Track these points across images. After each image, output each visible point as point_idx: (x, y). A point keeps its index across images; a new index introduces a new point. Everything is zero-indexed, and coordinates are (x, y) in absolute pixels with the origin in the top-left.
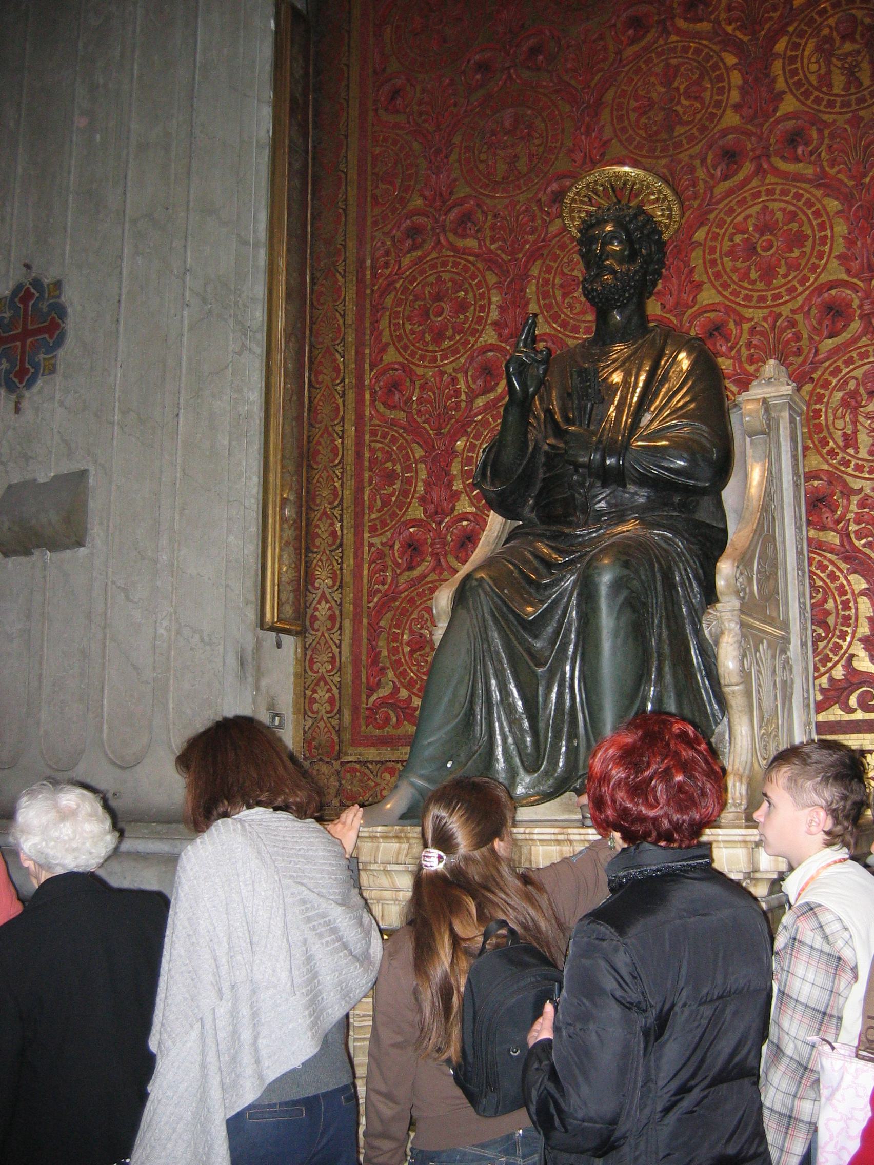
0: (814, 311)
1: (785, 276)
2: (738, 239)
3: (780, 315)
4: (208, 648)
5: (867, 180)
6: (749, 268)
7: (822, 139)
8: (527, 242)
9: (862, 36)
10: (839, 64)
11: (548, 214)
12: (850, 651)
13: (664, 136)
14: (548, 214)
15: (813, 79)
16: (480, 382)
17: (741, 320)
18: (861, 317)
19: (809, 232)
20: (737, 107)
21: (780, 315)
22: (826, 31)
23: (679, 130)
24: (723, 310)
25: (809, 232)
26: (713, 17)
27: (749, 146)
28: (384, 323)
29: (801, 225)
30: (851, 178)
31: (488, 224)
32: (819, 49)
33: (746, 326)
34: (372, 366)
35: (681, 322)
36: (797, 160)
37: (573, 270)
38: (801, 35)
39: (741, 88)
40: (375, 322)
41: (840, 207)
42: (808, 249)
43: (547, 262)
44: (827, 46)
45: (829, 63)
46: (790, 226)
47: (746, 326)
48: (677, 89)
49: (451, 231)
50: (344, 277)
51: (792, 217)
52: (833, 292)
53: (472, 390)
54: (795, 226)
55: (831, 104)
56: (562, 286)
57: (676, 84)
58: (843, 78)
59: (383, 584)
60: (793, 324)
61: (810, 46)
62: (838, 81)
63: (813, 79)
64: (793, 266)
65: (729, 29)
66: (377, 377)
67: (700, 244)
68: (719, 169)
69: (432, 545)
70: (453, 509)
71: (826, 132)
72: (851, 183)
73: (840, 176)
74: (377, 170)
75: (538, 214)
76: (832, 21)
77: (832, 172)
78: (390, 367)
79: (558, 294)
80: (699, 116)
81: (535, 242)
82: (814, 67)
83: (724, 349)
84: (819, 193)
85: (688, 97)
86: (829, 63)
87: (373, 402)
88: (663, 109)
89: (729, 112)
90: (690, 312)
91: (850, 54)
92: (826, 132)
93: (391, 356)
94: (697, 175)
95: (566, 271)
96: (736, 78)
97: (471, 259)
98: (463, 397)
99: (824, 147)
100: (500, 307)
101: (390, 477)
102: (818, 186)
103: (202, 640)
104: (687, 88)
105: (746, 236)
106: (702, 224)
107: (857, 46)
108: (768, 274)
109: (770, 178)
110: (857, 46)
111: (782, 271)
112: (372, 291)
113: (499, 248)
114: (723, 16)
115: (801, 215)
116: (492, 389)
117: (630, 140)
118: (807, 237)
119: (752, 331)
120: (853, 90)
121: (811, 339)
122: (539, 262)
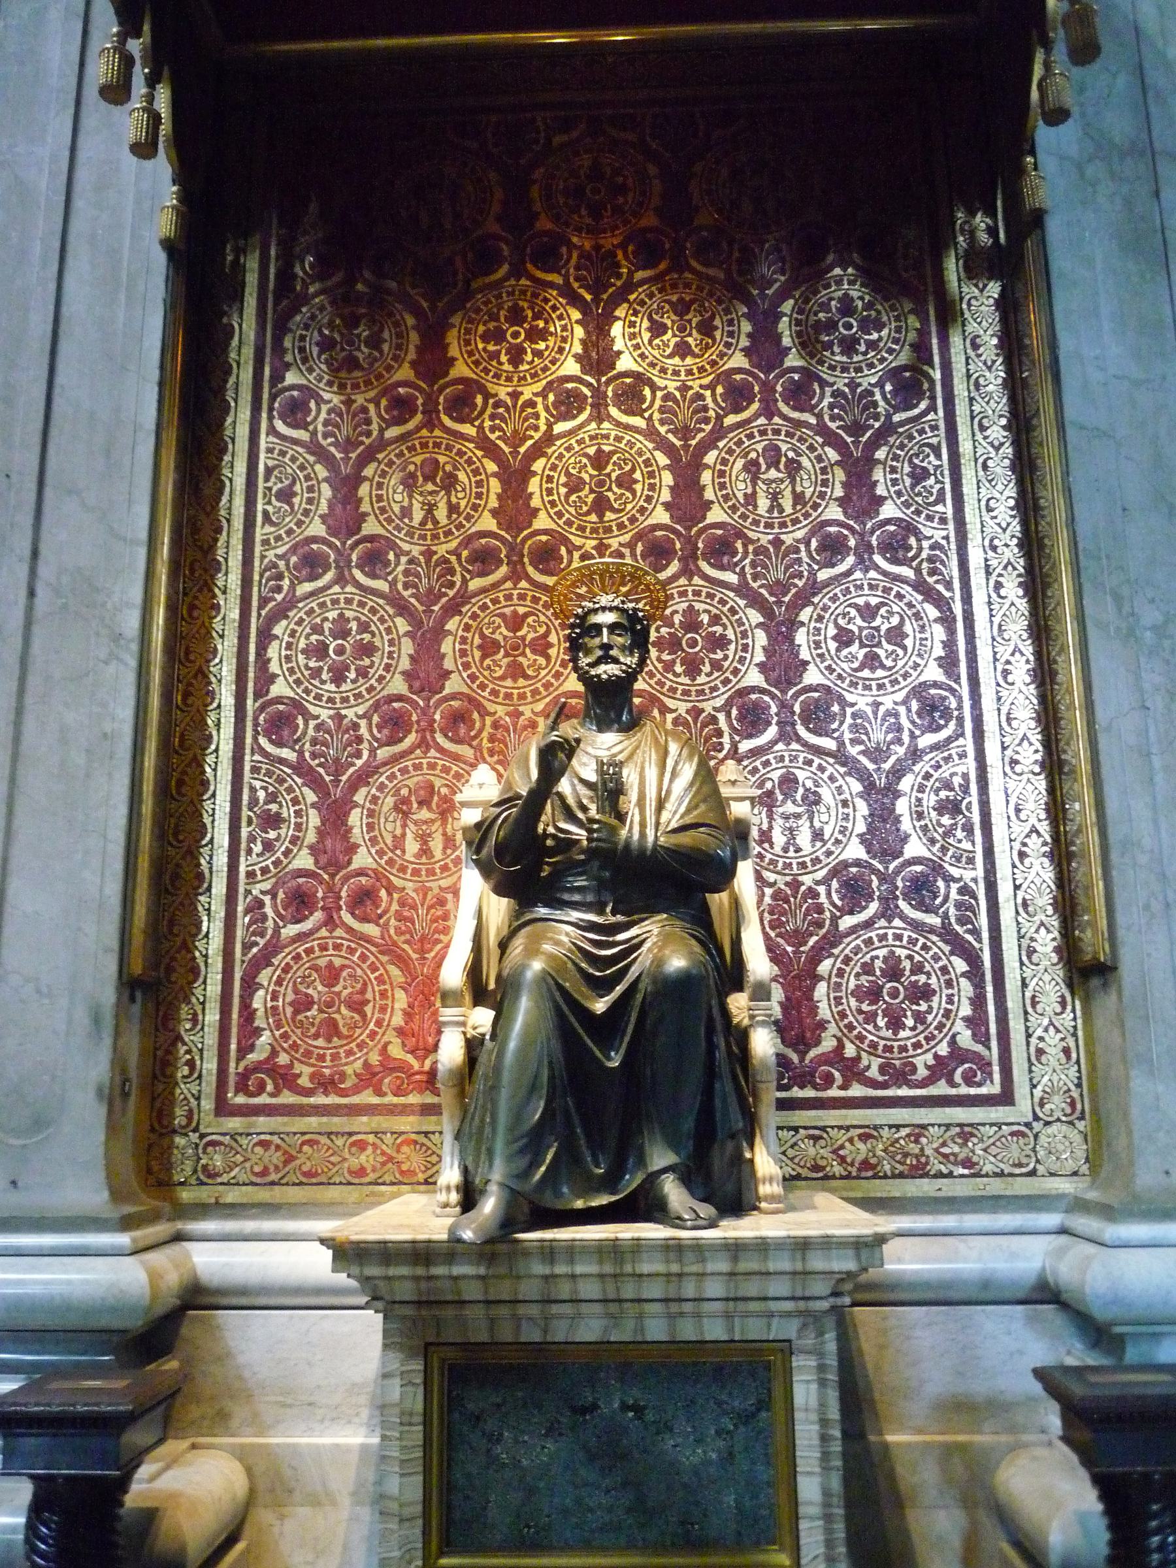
0: (734, 712)
1: (708, 675)
2: (664, 630)
3: (703, 711)
4: (46, 1001)
5: (786, 599)
6: (673, 662)
7: (746, 553)
8: (445, 595)
9: (786, 466)
10: (765, 487)
11: (468, 571)
12: (954, 1030)
13: (593, 518)
14: (468, 571)
15: (740, 496)
16: (386, 731)
18: (778, 723)
19: (733, 637)
20: (667, 506)
21: (703, 711)
22: (753, 455)
23: (609, 516)
25: (733, 637)
26: (646, 415)
27: (678, 546)
28: (273, 652)
29: (725, 628)
30: (771, 594)
31: (400, 568)
32: (746, 468)
33: (670, 717)
34: (257, 696)
36: (722, 568)
38: (730, 452)
39: (672, 489)
40: (262, 649)
41: (762, 620)
42: (731, 653)
43: (466, 620)
44: (754, 469)
45: (754, 484)
46: (714, 629)
47: (670, 717)
48: (609, 475)
49: (357, 567)
50: (224, 593)
51: (715, 620)
52: (753, 697)
53: (377, 740)
54: (718, 629)
55: (756, 523)
56: (480, 647)
59: (262, 937)
60: (713, 720)
61: (740, 463)
62: (763, 503)
63: (740, 496)
64: (716, 666)
65: (662, 430)
66: (262, 708)
69: (323, 899)
70: (349, 862)
71: (751, 548)
72: (772, 599)
73: (762, 591)
74: (269, 484)
75: (458, 569)
76: (759, 447)
77: (755, 585)
78: (279, 700)
79: (477, 654)
80: (629, 506)
81: (453, 598)
82: (742, 486)
84: (742, 603)
85: (619, 486)
86: (754, 484)
87: (256, 733)
89: (660, 509)
91: (774, 481)
92: (751, 548)
93: (279, 689)
95: (486, 632)
96: (668, 478)
97: (381, 602)
98: (365, 745)
99: (747, 561)
100: (411, 656)
101: (272, 821)
102: (742, 597)
103: (38, 991)
104: (618, 477)
107: (781, 475)
108: (693, 668)
109: (697, 580)
110: (781, 475)
111: (707, 668)
112: (259, 615)
113: (413, 595)
114: (656, 416)
115: (725, 620)
116: (401, 740)
117: (560, 515)
118: (730, 642)
119: (676, 722)
120: (776, 514)
121: (732, 738)
122: (457, 618)
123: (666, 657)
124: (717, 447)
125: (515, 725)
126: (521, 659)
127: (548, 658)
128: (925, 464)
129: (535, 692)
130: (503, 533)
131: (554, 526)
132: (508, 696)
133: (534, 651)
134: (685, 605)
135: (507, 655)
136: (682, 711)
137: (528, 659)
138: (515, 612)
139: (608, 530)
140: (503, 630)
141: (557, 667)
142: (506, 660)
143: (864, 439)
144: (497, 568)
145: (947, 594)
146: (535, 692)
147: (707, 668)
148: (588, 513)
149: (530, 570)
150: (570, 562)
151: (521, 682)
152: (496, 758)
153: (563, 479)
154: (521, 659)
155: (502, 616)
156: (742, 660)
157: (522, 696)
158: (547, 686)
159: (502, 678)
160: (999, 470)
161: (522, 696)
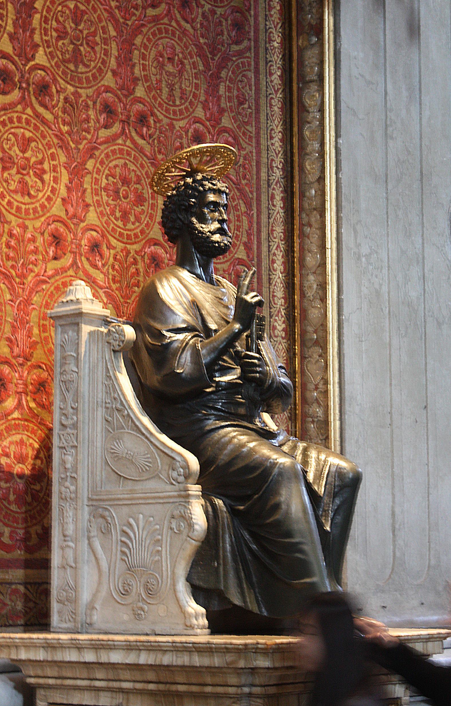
10: (166, 77)
13: (72, 67)
17: (110, 247)
24: (100, 232)
29: (143, 189)
35: (77, 230)
37: (10, 149)
45: (161, 74)
57: (80, 28)
58: (167, 89)
67: (89, 173)
68: (102, 117)
83: (100, 264)
88: (72, 43)
90: (82, 225)
94: (90, 113)
105: (115, 181)
106: (91, 157)
115: (143, 181)
123: (111, 202)
124: (141, 32)
125: (23, 236)
126: (27, 178)
127: (43, 181)
128: (244, 91)
129: (35, 210)
130: (16, 58)
131: (48, 65)
132: (18, 209)
133: (35, 174)
134: (122, 161)
135: (18, 172)
136: (118, 249)
137: (31, 180)
138: (23, 134)
139: (80, 81)
140: (16, 148)
141: (49, 193)
142: (18, 177)
143: (216, 58)
144: (13, 89)
145: (251, 196)
146: (35, 210)
147: (132, 219)
148: (69, 61)
149: (33, 99)
150: (58, 101)
151: (27, 199)
152: (10, 263)
153: (54, 24)
154: (27, 178)
155: (15, 135)
156: (151, 217)
157: (27, 211)
158: (43, 206)
159: (15, 192)
160: (276, 108)
161: (27, 211)
